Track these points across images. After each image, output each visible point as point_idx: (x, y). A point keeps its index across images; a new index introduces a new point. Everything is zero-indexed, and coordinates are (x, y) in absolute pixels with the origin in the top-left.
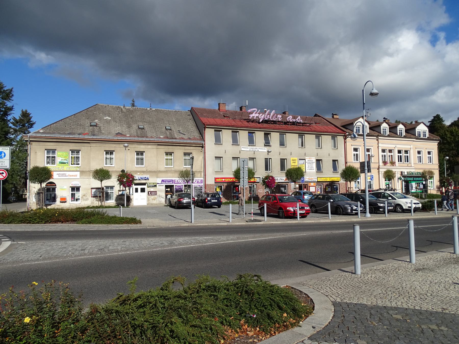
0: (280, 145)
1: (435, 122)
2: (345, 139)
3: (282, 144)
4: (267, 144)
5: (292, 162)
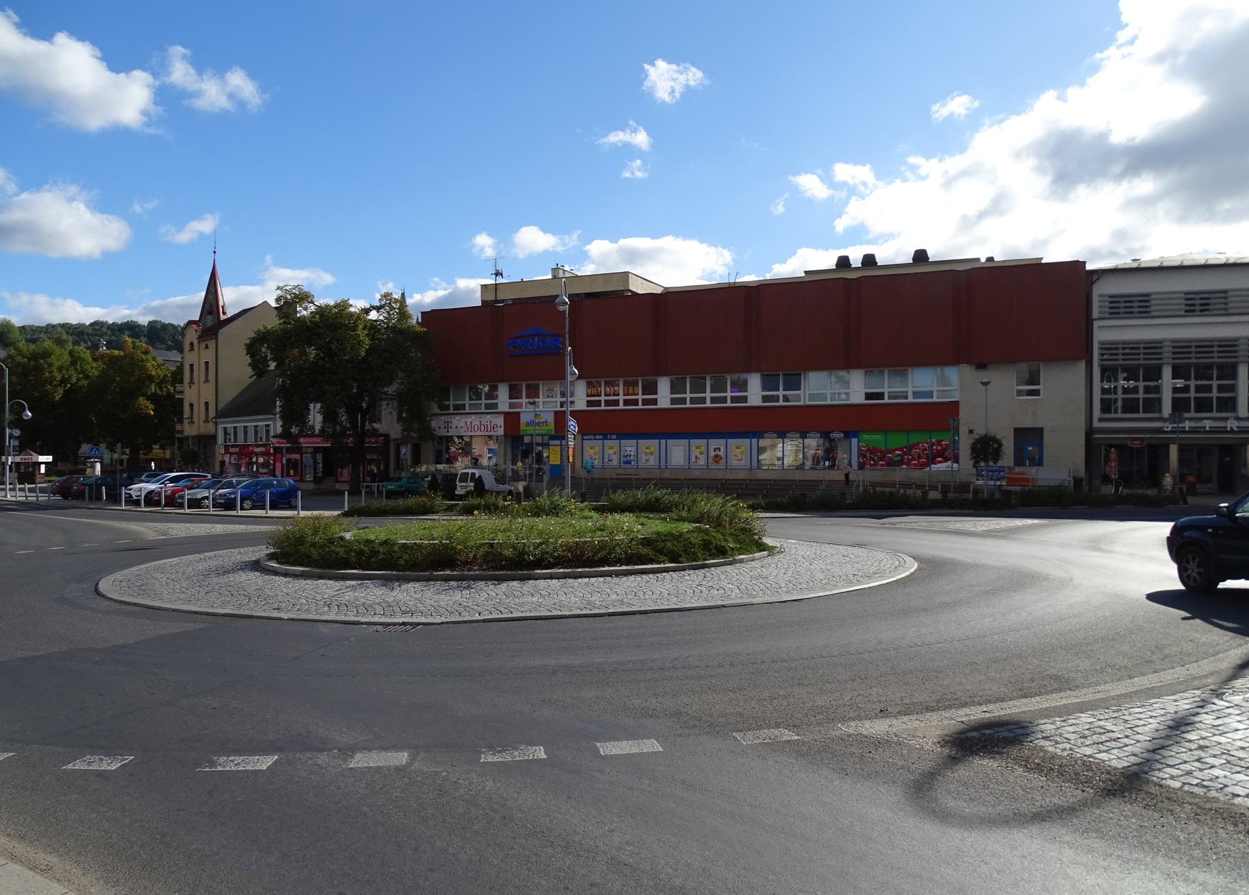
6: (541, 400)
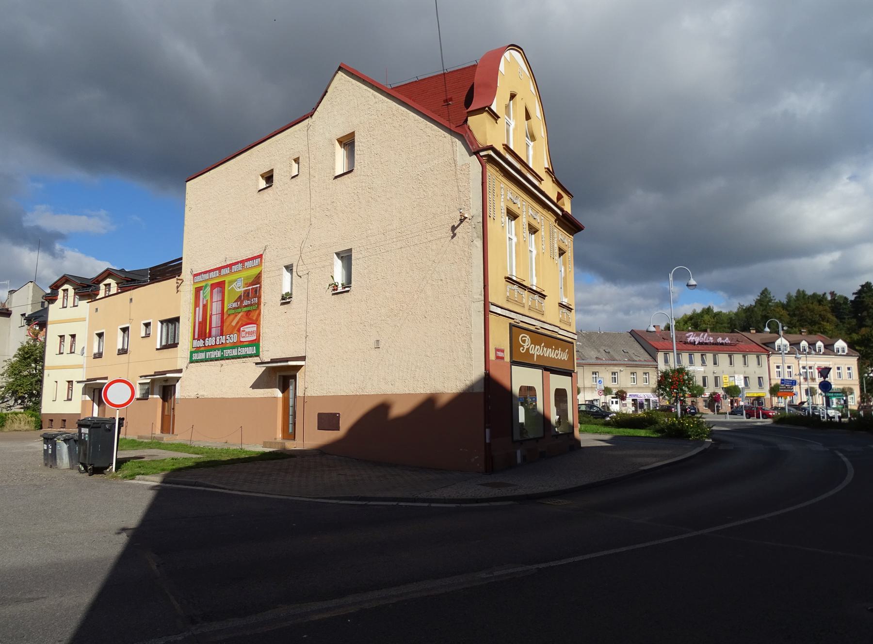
0: (714, 364)
1: (864, 295)
2: (768, 357)
3: (715, 363)
4: (703, 363)
5: (724, 379)
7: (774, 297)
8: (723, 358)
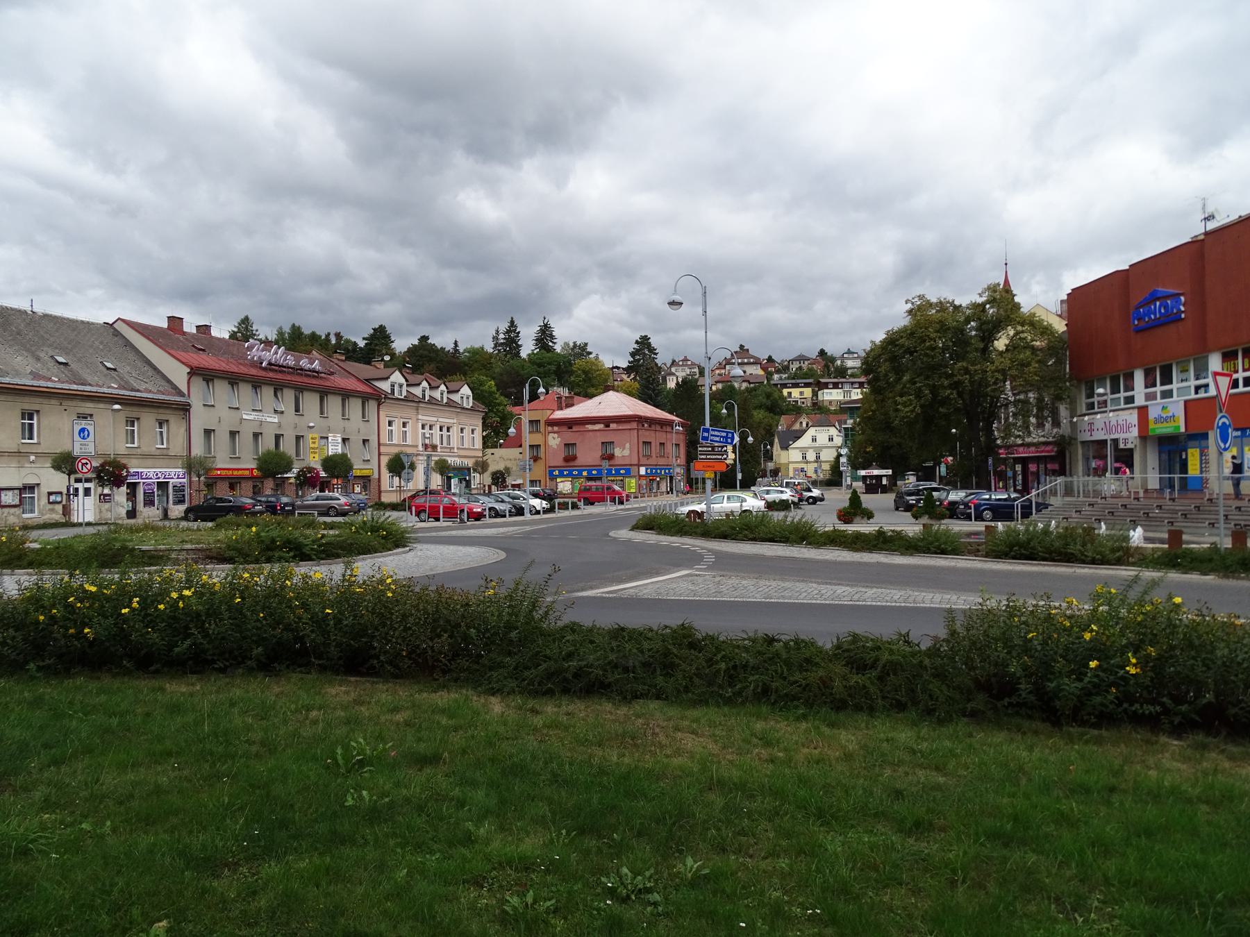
6: (1174, 386)
7: (257, 331)
8: (310, 402)
